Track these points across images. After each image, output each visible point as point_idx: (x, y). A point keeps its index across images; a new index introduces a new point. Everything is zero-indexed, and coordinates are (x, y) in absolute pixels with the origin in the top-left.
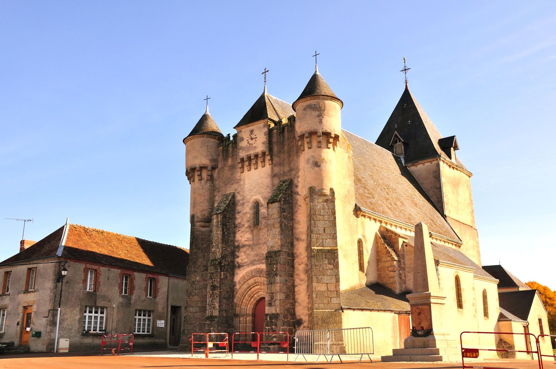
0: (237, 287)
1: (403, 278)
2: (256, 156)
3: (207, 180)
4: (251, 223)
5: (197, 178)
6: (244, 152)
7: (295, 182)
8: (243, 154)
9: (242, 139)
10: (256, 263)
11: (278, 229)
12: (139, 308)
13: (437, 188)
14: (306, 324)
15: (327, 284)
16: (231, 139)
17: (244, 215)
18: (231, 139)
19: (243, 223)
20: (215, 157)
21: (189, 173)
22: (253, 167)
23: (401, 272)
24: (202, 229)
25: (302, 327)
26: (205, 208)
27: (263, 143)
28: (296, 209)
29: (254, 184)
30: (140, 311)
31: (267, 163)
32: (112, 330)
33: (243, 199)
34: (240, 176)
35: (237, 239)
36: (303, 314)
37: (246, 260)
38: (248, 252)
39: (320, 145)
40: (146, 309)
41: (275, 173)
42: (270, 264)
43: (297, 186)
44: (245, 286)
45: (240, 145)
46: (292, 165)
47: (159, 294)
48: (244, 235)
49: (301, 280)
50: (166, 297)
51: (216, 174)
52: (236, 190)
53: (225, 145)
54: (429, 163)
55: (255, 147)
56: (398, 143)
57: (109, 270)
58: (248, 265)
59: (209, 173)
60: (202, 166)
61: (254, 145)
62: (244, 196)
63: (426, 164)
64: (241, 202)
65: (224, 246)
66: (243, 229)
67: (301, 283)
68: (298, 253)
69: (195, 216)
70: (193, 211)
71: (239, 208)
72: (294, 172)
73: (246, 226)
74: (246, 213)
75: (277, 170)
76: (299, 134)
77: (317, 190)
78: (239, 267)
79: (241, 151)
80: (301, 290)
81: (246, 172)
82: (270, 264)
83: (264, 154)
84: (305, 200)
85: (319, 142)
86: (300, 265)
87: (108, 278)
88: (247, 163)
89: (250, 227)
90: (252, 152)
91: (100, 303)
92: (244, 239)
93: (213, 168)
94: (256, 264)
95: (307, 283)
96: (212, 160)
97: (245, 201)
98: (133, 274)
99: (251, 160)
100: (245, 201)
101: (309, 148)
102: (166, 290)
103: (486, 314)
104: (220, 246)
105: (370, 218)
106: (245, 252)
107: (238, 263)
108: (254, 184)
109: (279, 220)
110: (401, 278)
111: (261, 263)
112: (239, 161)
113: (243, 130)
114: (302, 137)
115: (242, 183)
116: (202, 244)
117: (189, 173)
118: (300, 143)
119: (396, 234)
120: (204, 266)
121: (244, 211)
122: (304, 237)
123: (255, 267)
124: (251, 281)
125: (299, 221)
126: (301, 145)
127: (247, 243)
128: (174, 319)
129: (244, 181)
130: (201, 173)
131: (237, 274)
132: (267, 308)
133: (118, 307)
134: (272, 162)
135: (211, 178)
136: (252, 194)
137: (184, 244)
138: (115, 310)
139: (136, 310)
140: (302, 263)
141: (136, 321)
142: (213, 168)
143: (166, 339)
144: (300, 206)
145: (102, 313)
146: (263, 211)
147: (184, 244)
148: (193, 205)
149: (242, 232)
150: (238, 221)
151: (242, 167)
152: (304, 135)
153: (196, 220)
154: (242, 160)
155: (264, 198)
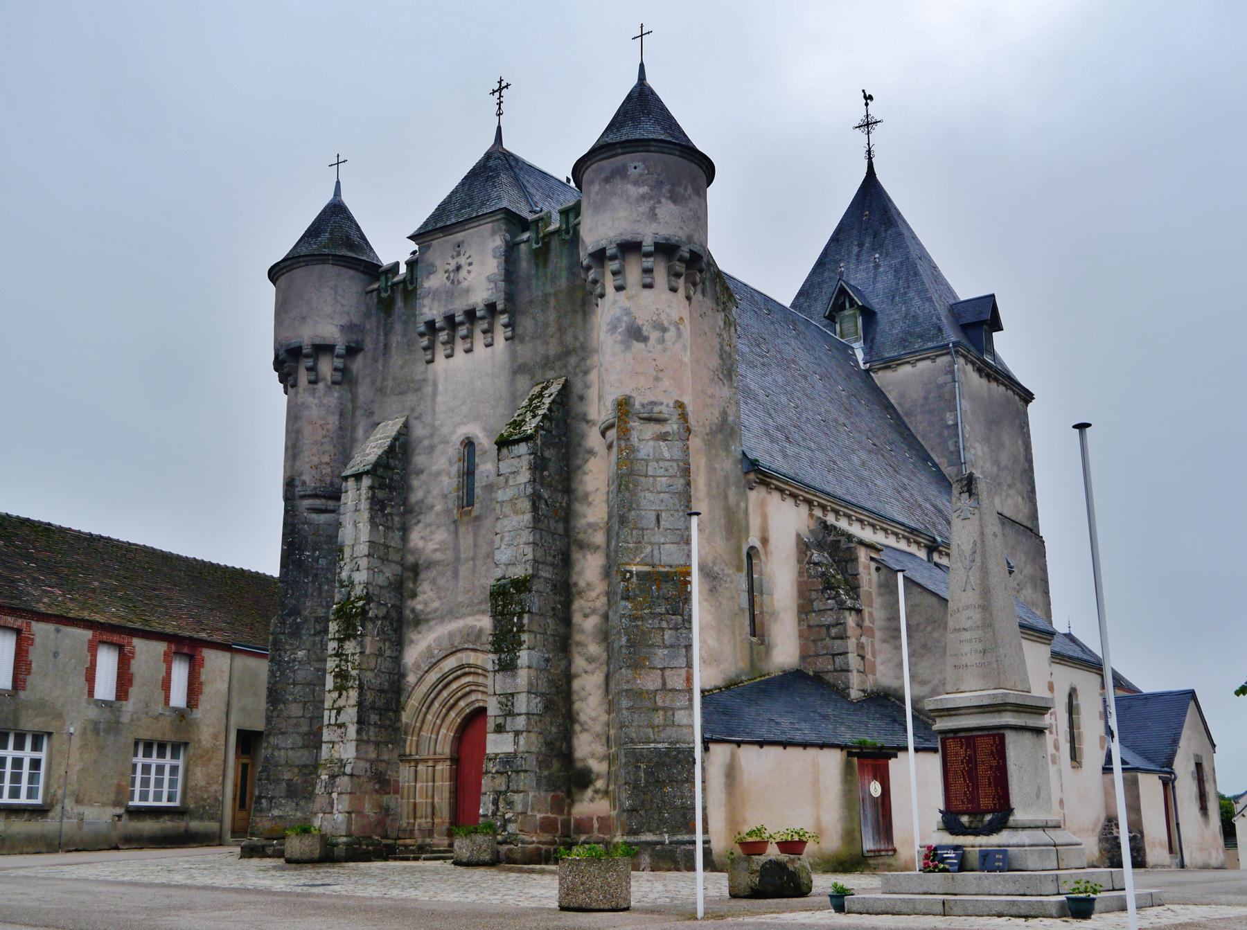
0: (411, 679)
1: (869, 656)
2: (471, 315)
3: (334, 383)
4: (452, 503)
5: (303, 377)
6: (436, 303)
7: (578, 386)
8: (431, 310)
9: (431, 271)
10: (464, 610)
11: (528, 517)
12: (145, 735)
13: (948, 427)
14: (600, 784)
15: (663, 669)
16: (403, 269)
17: (435, 477)
18: (403, 269)
19: (430, 500)
20: (355, 320)
21: (283, 362)
22: (460, 346)
23: (863, 639)
24: (314, 516)
25: (589, 793)
26: (326, 459)
27: (489, 279)
28: (579, 462)
29: (466, 391)
30: (148, 746)
31: (500, 335)
32: (64, 796)
33: (432, 435)
34: (426, 371)
35: (412, 544)
36: (593, 755)
37: (436, 604)
38: (441, 582)
39: (648, 280)
40: (166, 738)
41: (520, 361)
42: (502, 614)
43: (581, 398)
44: (433, 676)
45: (426, 284)
46: (569, 339)
47: (202, 698)
48: (432, 533)
49: (590, 660)
50: (224, 709)
51: (358, 364)
52: (413, 410)
53: (390, 292)
54: (928, 362)
55: (467, 291)
56: (848, 312)
57: (58, 631)
58: (442, 619)
59: (339, 363)
60: (318, 341)
61: (465, 284)
63: (921, 365)
64: (426, 443)
65: (377, 563)
66: (429, 518)
67: (590, 668)
68: (582, 584)
69: (297, 483)
70: (292, 466)
71: (419, 460)
72: (573, 360)
73: (438, 508)
74: (439, 474)
75: (526, 352)
76: (591, 249)
77: (637, 406)
78: (418, 621)
79: (427, 301)
80: (588, 688)
81: (441, 361)
82: (502, 614)
83: (491, 308)
84: (603, 434)
86: (586, 616)
87: (55, 655)
88: (443, 336)
89: (447, 511)
90: (458, 307)
91: (30, 723)
92: (431, 546)
93: (352, 351)
94: (464, 616)
95: (605, 668)
96: (349, 328)
98: (130, 644)
99: (458, 326)
100: (436, 440)
101: (619, 288)
102: (225, 686)
103: (1075, 755)
104: (363, 563)
105: (782, 491)
106: (434, 582)
107: (413, 610)
108: (466, 391)
109: (529, 490)
110: (863, 658)
112: (422, 328)
113: (434, 243)
114: (600, 256)
115: (428, 389)
116: (317, 560)
117: (283, 362)
118: (592, 275)
119: (849, 537)
120: (317, 619)
121: (435, 468)
122: (599, 538)
124: (451, 663)
125: (586, 496)
126: (595, 282)
127: (438, 556)
128: (245, 767)
129: (435, 385)
130: (316, 363)
131: (412, 641)
132: (491, 737)
133: (84, 732)
134: (513, 330)
135: (345, 378)
137: (268, 562)
138: (76, 742)
139: (136, 744)
140: (594, 611)
141: (134, 771)
142: (352, 351)
143: (221, 821)
144: (591, 452)
145: (36, 747)
146: (485, 468)
147: (268, 562)
148: (293, 450)
149: (426, 527)
150: (416, 496)
151: (430, 348)
152: (603, 250)
153: (299, 490)
154: (431, 325)
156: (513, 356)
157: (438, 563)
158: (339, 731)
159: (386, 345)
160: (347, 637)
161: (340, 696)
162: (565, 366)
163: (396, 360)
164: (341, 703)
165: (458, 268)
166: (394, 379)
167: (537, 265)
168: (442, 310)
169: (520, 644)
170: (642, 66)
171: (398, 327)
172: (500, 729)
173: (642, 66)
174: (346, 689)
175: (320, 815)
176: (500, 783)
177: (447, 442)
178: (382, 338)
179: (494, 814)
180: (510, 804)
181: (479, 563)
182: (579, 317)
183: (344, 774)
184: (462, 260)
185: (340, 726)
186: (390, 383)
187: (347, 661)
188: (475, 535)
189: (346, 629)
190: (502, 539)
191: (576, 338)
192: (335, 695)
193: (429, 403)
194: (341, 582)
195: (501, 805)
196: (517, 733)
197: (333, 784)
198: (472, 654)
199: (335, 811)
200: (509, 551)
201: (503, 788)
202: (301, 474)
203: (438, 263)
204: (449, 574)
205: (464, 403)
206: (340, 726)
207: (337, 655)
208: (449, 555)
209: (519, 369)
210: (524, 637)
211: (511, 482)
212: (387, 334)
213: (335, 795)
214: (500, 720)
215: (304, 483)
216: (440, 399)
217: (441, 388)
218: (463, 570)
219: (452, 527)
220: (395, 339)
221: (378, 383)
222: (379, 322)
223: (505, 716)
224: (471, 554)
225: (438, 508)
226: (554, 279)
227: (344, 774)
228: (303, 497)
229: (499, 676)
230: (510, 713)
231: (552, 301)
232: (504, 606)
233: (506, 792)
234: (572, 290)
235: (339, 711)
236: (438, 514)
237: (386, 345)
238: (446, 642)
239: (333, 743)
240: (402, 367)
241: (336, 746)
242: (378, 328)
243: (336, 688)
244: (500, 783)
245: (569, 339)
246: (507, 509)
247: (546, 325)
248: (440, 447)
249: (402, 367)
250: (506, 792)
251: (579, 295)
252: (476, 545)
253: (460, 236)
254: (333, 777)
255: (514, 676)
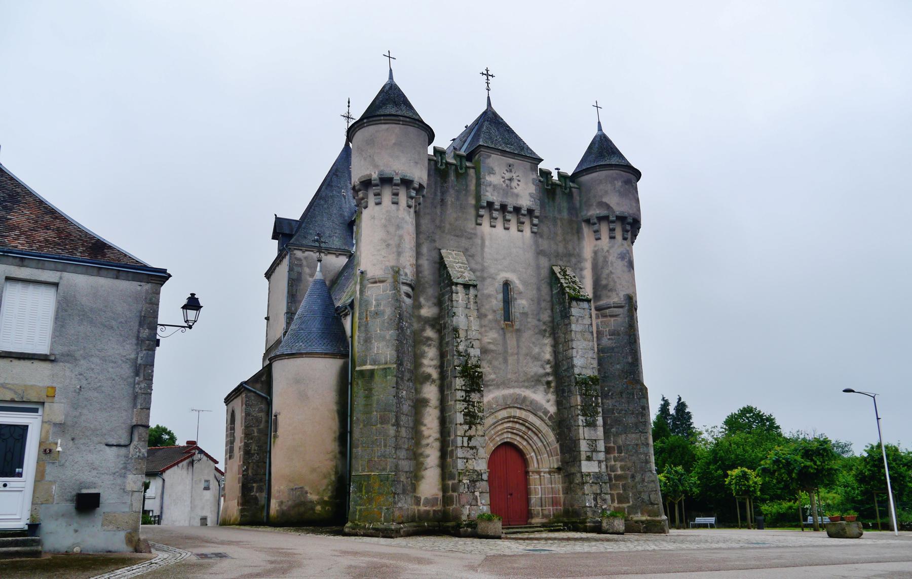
2: (517, 210)
33: (482, 270)
34: (475, 229)
37: (493, 376)
38: (496, 363)
55: (517, 195)
58: (498, 386)
61: (515, 191)
62: (482, 265)
69: (402, 273)
72: (574, 260)
74: (489, 296)
81: (486, 226)
83: (530, 212)
85: (612, 230)
89: (496, 321)
90: (511, 203)
94: (513, 387)
97: (485, 275)
106: (490, 362)
111: (523, 386)
123: (511, 391)
124: (504, 414)
127: (491, 347)
132: (584, 463)
136: (500, 267)
153: (402, 278)
155: (524, 283)
156: (536, 244)
157: (492, 351)
158: (471, 451)
159: (442, 200)
160: (473, 390)
161: (470, 428)
162: (569, 261)
163: (451, 214)
164: (472, 432)
165: (511, 180)
166: (450, 224)
167: (548, 198)
168: (500, 199)
169: (597, 413)
170: (599, 123)
171: (452, 191)
172: (589, 459)
173: (599, 123)
174: (475, 424)
175: (468, 507)
176: (596, 489)
177: (494, 279)
178: (439, 194)
179: (596, 506)
180: (604, 500)
181: (521, 358)
182: (575, 238)
183: (482, 480)
184: (515, 176)
185: (472, 448)
186: (447, 226)
187: (474, 406)
188: (518, 341)
189: (472, 385)
190: (577, 352)
191: (574, 249)
192: (467, 427)
193: (479, 249)
194: (458, 352)
195: (599, 501)
196: (600, 462)
197: (474, 487)
198: (518, 411)
199: (479, 503)
200: (582, 360)
201: (599, 492)
202: (404, 268)
203: (497, 169)
204: (501, 359)
205: (504, 258)
206: (472, 448)
207: (464, 401)
208: (500, 348)
209: (540, 253)
210: (600, 410)
211: (580, 321)
212: (443, 193)
213: (477, 494)
214: (589, 454)
215: (406, 275)
216: (486, 250)
217: (487, 243)
218: (511, 360)
219: (501, 332)
220: (450, 199)
221: (437, 222)
222: (436, 183)
223: (592, 452)
224: (516, 351)
225: (490, 317)
226: (560, 211)
227: (482, 480)
228: (403, 283)
229: (586, 429)
230: (595, 450)
231: (559, 223)
232: (586, 390)
233: (600, 494)
234: (570, 222)
235: (470, 438)
236: (490, 321)
237: (442, 200)
238: (501, 401)
239: (467, 459)
240: (456, 220)
241: (470, 462)
242: (436, 187)
243: (466, 423)
244: (596, 489)
245: (570, 247)
246: (579, 336)
247: (556, 234)
248: (489, 280)
249: (456, 220)
250: (600, 494)
251: (575, 226)
252: (518, 347)
253: (511, 161)
254: (473, 481)
255: (595, 430)
